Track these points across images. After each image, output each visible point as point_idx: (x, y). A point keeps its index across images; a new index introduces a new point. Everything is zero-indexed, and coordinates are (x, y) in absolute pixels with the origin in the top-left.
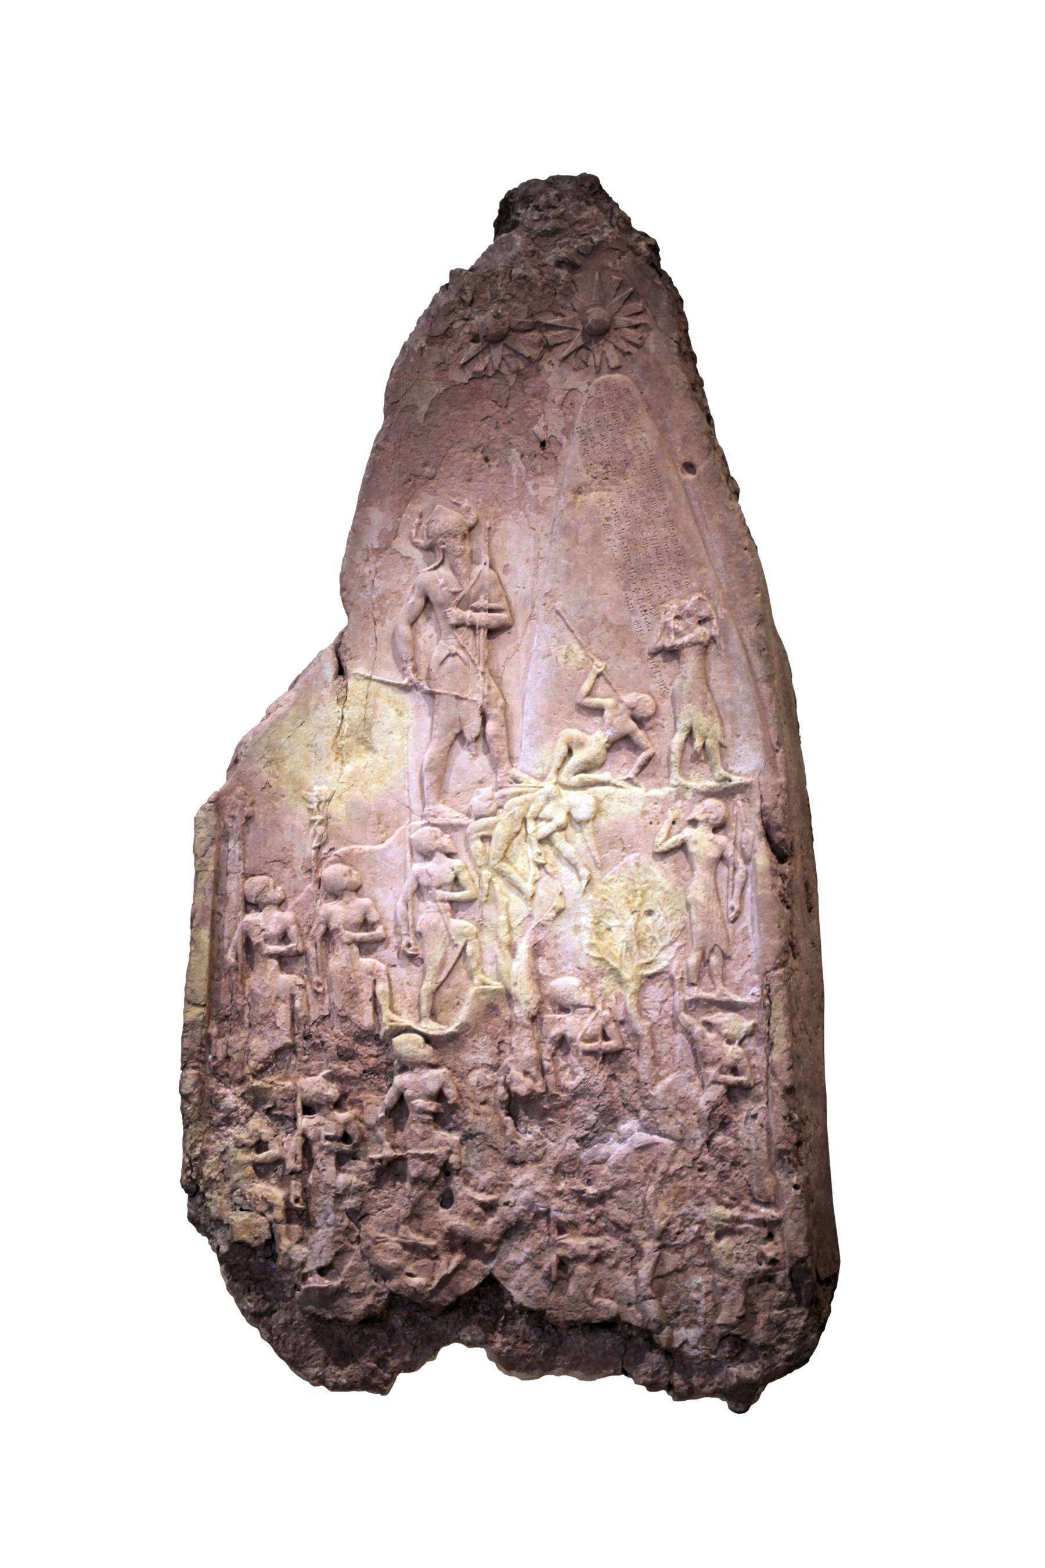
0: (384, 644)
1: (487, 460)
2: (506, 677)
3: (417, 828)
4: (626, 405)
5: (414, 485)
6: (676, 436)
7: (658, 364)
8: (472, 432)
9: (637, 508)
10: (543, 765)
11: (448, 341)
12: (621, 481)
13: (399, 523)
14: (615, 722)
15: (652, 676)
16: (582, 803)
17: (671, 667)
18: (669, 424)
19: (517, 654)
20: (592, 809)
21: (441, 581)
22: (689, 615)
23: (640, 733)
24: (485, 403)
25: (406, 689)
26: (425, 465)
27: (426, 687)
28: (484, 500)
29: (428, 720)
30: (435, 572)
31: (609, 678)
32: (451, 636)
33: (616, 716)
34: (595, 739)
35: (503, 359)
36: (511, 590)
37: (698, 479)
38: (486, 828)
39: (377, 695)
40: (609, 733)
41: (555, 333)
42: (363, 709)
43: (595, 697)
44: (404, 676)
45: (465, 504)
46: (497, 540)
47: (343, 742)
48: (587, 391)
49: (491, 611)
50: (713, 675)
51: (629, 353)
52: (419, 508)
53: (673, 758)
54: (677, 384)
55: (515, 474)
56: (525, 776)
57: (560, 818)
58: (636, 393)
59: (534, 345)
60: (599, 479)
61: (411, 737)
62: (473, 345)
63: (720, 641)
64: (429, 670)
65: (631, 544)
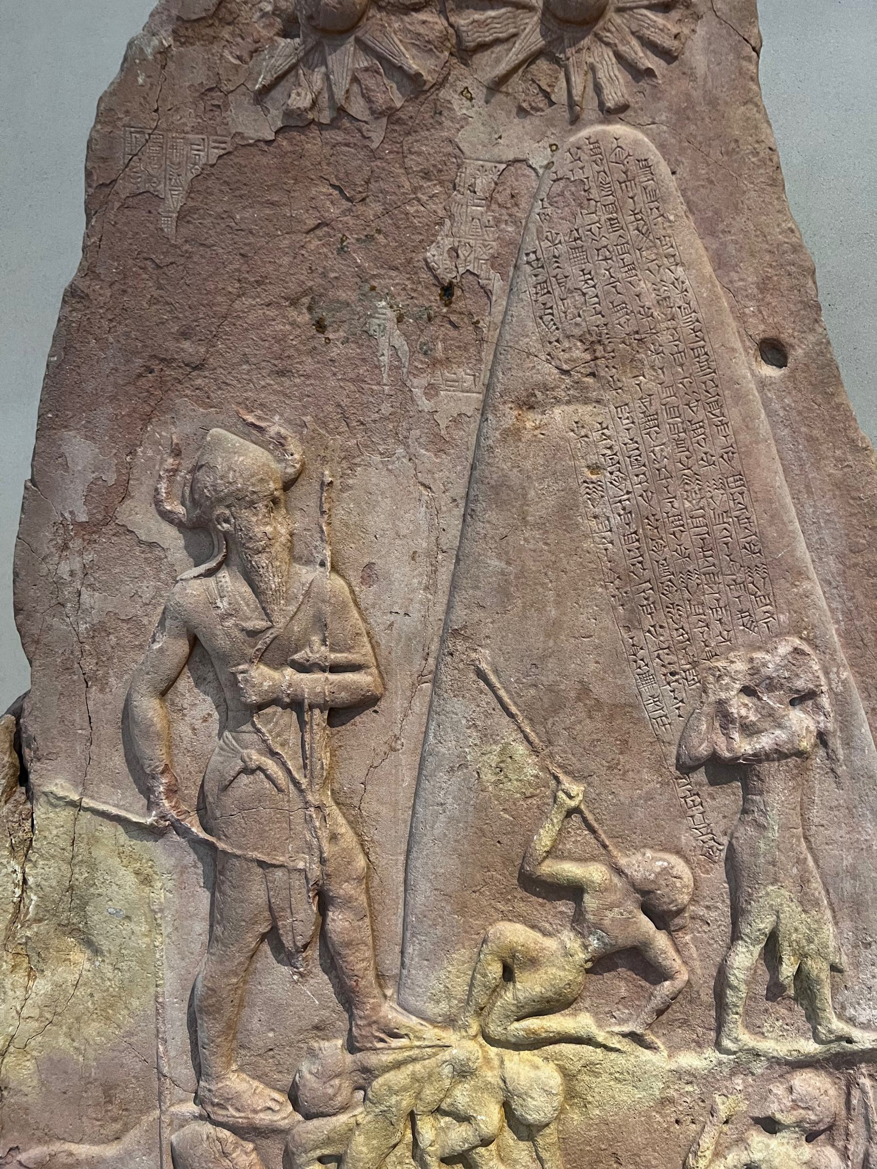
0: (110, 731)
1: (320, 326)
2: (371, 806)
3: (183, 1122)
4: (641, 199)
5: (162, 382)
6: (748, 276)
7: (713, 103)
8: (286, 260)
9: (661, 446)
10: (449, 997)
11: (226, 33)
12: (627, 381)
13: (130, 467)
14: (607, 922)
15: (684, 814)
16: (535, 1077)
17: (728, 797)
18: (731, 248)
19: (392, 756)
20: (557, 1101)
21: (223, 604)
22: (772, 685)
23: (661, 940)
24: (313, 192)
25: (154, 832)
26: (185, 335)
27: (197, 830)
28: (316, 418)
29: (205, 897)
30: (211, 582)
31: (590, 817)
32: (247, 727)
33: (610, 908)
34: (559, 952)
35: (355, 80)
36: (379, 620)
37: (792, 377)
38: (329, 1141)
39: (93, 840)
40: (594, 943)
41: (477, 16)
42: (65, 867)
43: (562, 858)
44: (151, 806)
45: (276, 427)
46: (343, 510)
47: (28, 934)
48: (547, 167)
49: (335, 668)
50: (816, 814)
51: (650, 73)
52: (175, 433)
53: (731, 997)
54: (756, 153)
55: (385, 359)
56: (413, 1021)
57: (490, 1117)
58: (663, 169)
59: (427, 47)
60: (576, 376)
61: (167, 929)
62: (282, 42)
63: (836, 743)
64: (202, 794)
65: (645, 525)
